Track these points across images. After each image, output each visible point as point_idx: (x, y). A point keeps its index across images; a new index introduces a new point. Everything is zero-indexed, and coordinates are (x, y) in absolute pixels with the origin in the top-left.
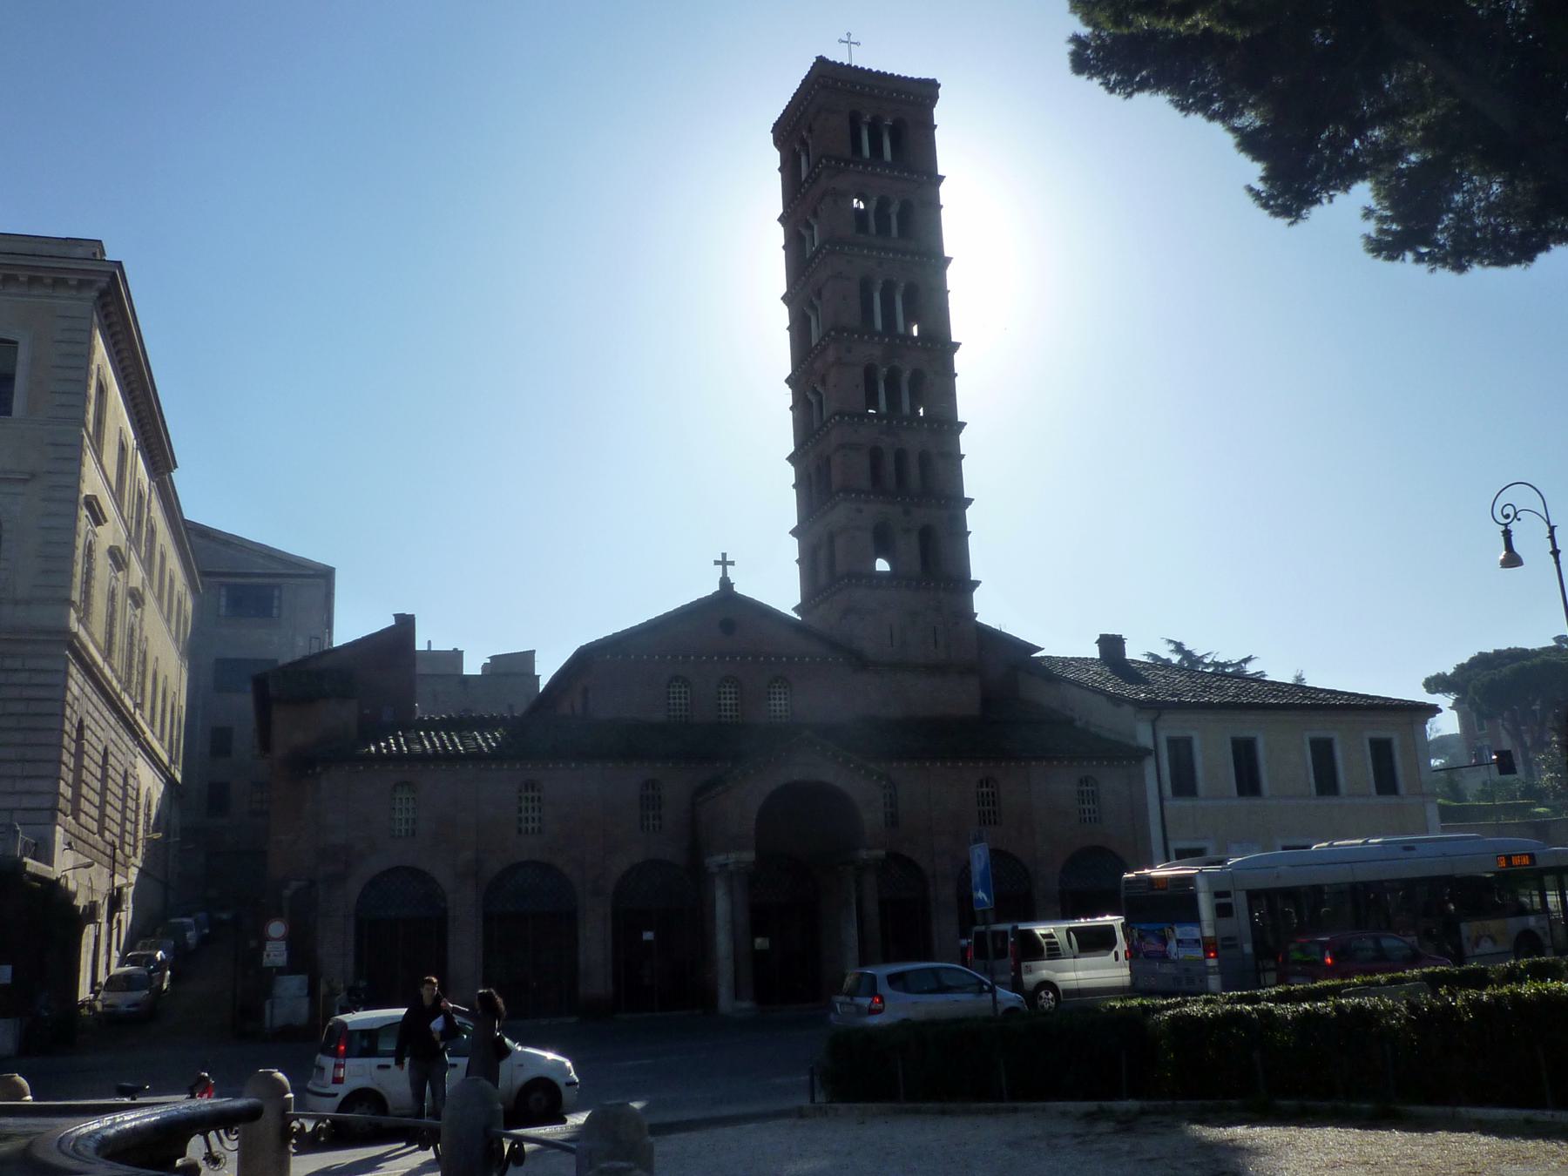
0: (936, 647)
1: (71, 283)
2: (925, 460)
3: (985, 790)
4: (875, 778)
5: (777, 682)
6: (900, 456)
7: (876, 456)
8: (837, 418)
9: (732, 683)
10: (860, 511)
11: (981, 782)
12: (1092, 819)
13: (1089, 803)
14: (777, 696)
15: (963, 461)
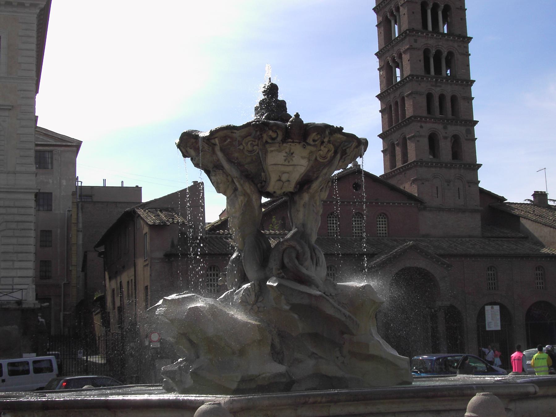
0: (459, 199)
1: (26, 5)
2: (454, 99)
3: (490, 272)
4: (445, 266)
5: (381, 215)
6: (442, 98)
7: (429, 97)
8: (410, 78)
9: (359, 215)
10: (421, 127)
11: (488, 268)
12: (541, 288)
13: (540, 279)
14: (381, 223)
15: (473, 101)
